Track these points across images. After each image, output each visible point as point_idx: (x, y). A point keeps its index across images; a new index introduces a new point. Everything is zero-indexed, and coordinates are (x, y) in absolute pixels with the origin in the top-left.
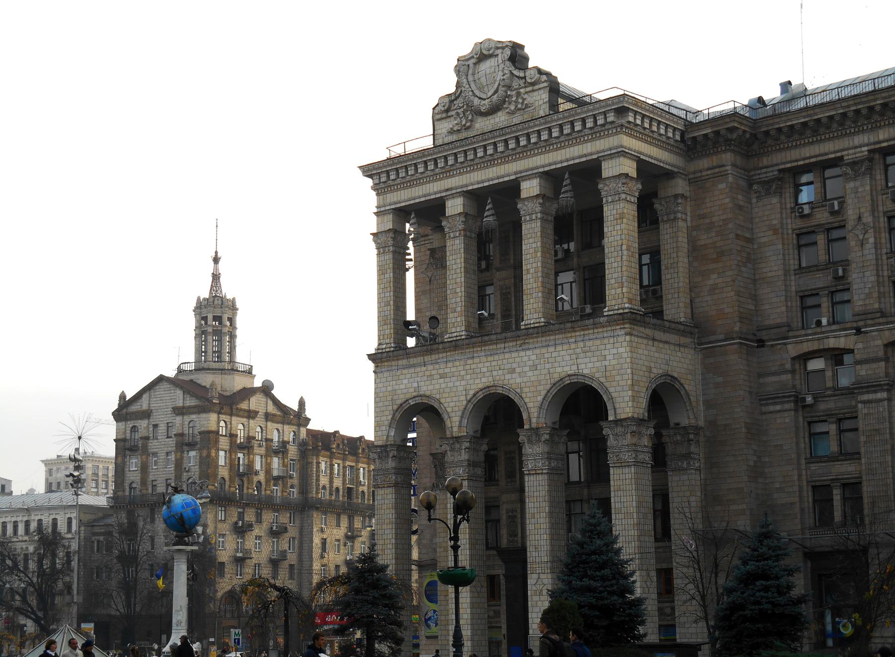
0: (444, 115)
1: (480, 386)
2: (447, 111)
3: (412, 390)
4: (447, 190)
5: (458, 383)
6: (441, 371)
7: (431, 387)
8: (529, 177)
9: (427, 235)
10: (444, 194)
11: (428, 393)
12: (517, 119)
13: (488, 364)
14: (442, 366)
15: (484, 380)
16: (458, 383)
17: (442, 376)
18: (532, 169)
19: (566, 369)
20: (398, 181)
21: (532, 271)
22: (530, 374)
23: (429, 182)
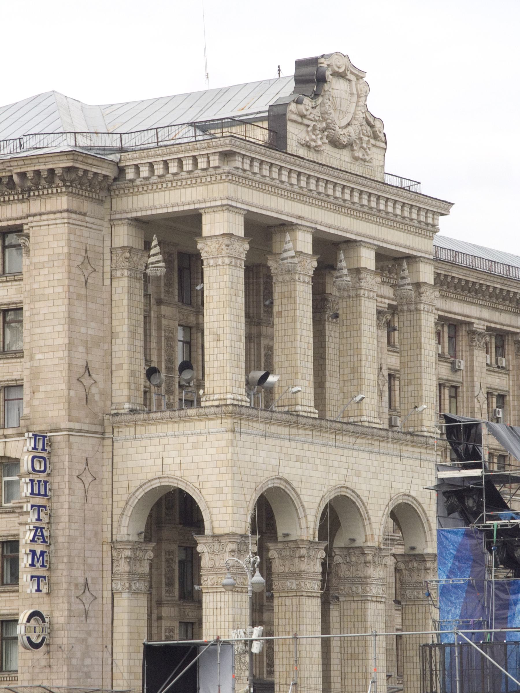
0: (299, 119)
1: (333, 483)
2: (303, 116)
3: (270, 468)
4: (299, 217)
5: (312, 473)
6: (297, 452)
7: (288, 470)
8: (368, 245)
9: (85, 215)
10: (295, 221)
11: (286, 476)
12: (358, 169)
13: (338, 458)
14: (299, 445)
15: (335, 477)
16: (312, 473)
17: (299, 460)
18: (370, 238)
19: (400, 485)
20: (258, 177)
21: (370, 358)
22: (372, 482)
23: (282, 196)
